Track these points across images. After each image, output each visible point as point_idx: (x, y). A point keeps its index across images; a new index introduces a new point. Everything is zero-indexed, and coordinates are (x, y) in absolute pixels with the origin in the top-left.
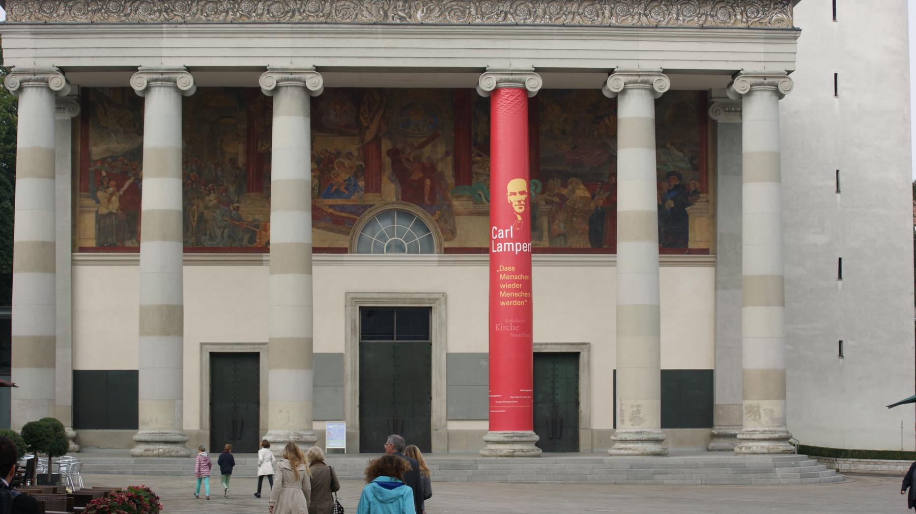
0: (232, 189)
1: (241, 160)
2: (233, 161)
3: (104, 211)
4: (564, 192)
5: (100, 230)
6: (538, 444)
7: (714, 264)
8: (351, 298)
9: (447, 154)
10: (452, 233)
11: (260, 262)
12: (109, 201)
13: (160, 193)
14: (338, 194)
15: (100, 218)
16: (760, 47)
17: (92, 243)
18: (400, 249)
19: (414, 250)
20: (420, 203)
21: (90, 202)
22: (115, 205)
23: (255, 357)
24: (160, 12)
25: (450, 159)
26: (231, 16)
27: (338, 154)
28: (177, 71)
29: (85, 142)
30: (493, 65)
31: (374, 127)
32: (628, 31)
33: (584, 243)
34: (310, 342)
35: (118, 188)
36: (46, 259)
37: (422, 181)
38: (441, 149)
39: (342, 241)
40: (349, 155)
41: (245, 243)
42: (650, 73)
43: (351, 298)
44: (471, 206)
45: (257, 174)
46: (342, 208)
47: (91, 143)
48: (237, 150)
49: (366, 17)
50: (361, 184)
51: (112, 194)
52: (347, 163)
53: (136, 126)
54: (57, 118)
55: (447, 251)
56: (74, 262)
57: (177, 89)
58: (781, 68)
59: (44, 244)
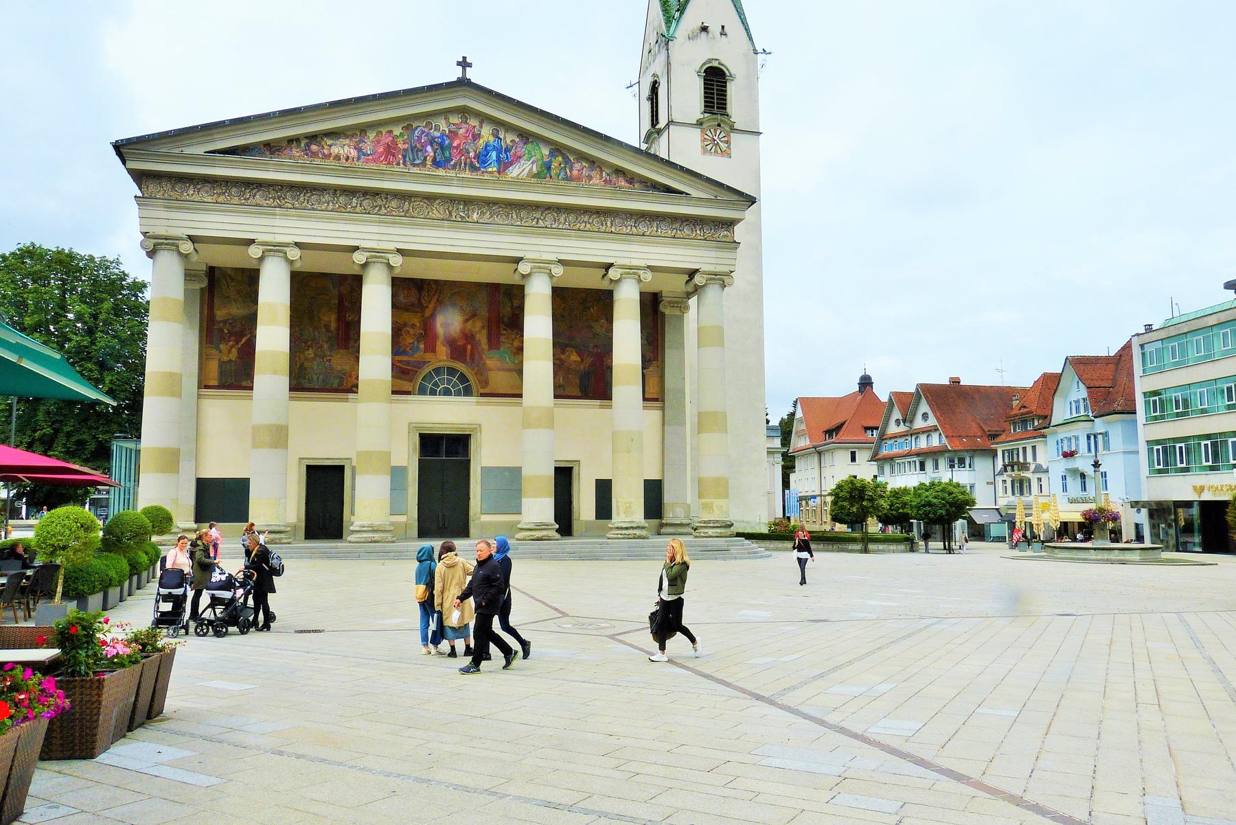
0: (326, 346)
1: (333, 326)
2: (327, 327)
3: (225, 359)
4: (563, 357)
5: (223, 372)
6: (557, 531)
7: (663, 409)
8: (412, 426)
9: (483, 328)
10: (485, 383)
11: (346, 400)
12: (230, 351)
13: (273, 336)
14: (404, 353)
15: (222, 364)
16: (714, 254)
17: (215, 383)
18: (447, 392)
19: (458, 394)
20: (464, 361)
21: (214, 352)
22: (234, 355)
23: (341, 469)
24: (274, 199)
25: (485, 332)
26: (331, 207)
27: (405, 325)
28: (287, 245)
29: (211, 307)
30: (528, 255)
31: (431, 306)
32: (624, 237)
33: (576, 392)
34: (388, 455)
35: (237, 342)
36: (172, 385)
37: (465, 345)
38: (478, 324)
39: (407, 386)
40: (413, 326)
41: (335, 385)
42: (638, 268)
43: (412, 426)
44: (498, 363)
45: (347, 334)
46: (408, 363)
47: (216, 307)
48: (331, 319)
49: (435, 214)
50: (422, 346)
51: (232, 347)
52: (412, 331)
53: (253, 297)
54: (190, 287)
55: (482, 395)
56: (199, 396)
57: (287, 260)
58: (726, 269)
59: (172, 375)
